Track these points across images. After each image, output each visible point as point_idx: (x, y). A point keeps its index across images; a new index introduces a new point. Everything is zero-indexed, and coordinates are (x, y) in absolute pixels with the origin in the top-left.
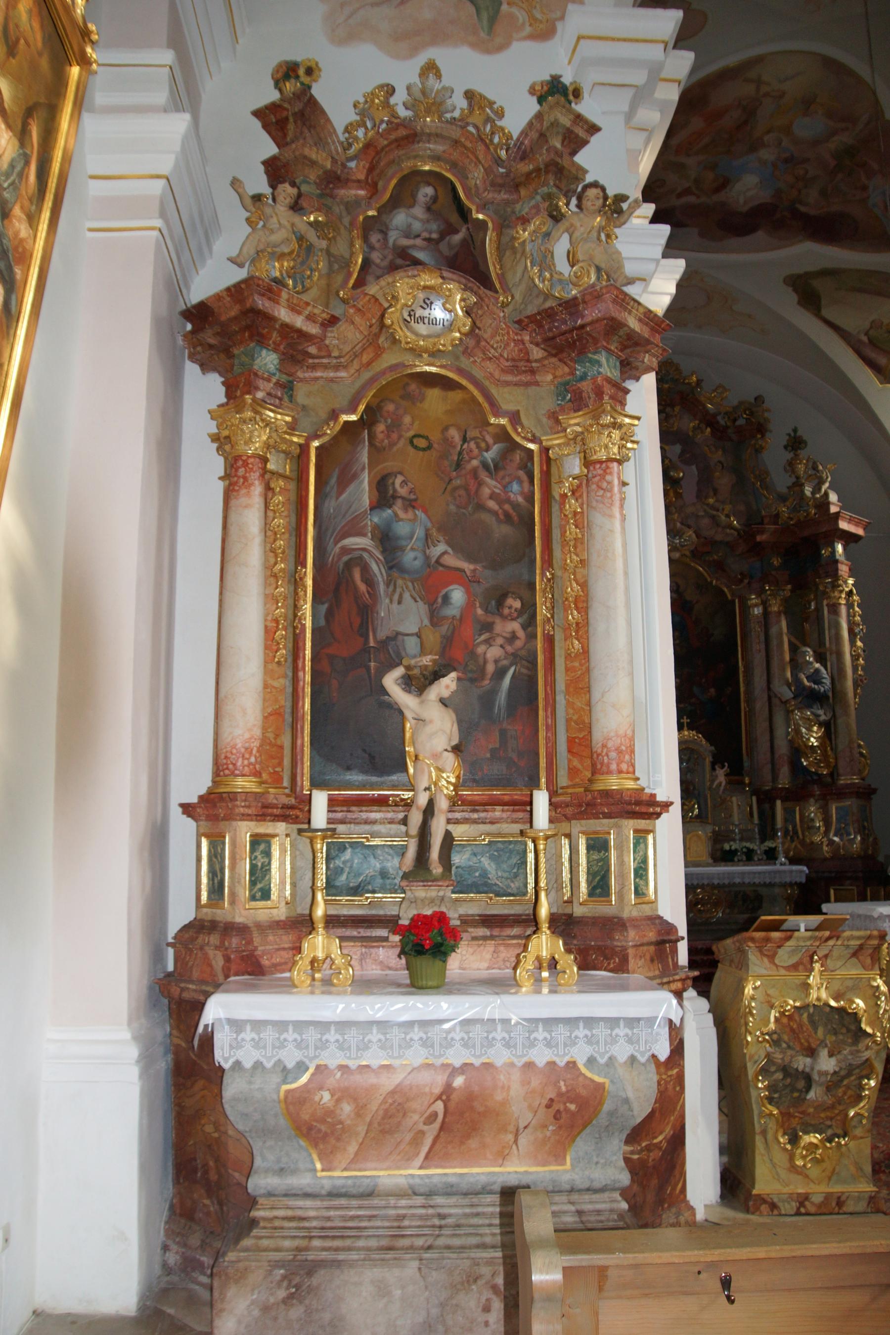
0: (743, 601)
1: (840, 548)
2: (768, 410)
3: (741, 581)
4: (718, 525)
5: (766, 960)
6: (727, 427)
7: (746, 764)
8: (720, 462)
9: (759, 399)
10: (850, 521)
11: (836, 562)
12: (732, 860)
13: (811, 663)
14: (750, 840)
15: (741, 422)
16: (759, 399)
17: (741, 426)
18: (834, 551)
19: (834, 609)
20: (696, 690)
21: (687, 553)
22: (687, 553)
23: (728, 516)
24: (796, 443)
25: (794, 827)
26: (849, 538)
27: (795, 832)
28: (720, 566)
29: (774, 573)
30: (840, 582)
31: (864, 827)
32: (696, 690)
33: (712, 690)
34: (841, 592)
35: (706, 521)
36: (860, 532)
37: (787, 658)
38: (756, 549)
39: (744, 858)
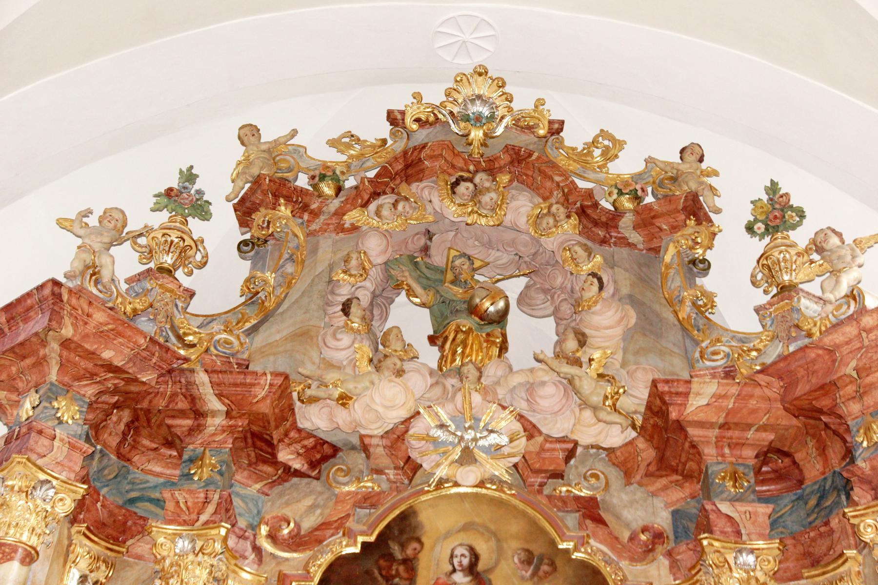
2: (716, 174)
3: (649, 551)
6: (617, 214)
8: (594, 275)
9: (692, 153)
15: (649, 199)
16: (692, 153)
17: (649, 207)
24: (775, 215)
29: (725, 508)
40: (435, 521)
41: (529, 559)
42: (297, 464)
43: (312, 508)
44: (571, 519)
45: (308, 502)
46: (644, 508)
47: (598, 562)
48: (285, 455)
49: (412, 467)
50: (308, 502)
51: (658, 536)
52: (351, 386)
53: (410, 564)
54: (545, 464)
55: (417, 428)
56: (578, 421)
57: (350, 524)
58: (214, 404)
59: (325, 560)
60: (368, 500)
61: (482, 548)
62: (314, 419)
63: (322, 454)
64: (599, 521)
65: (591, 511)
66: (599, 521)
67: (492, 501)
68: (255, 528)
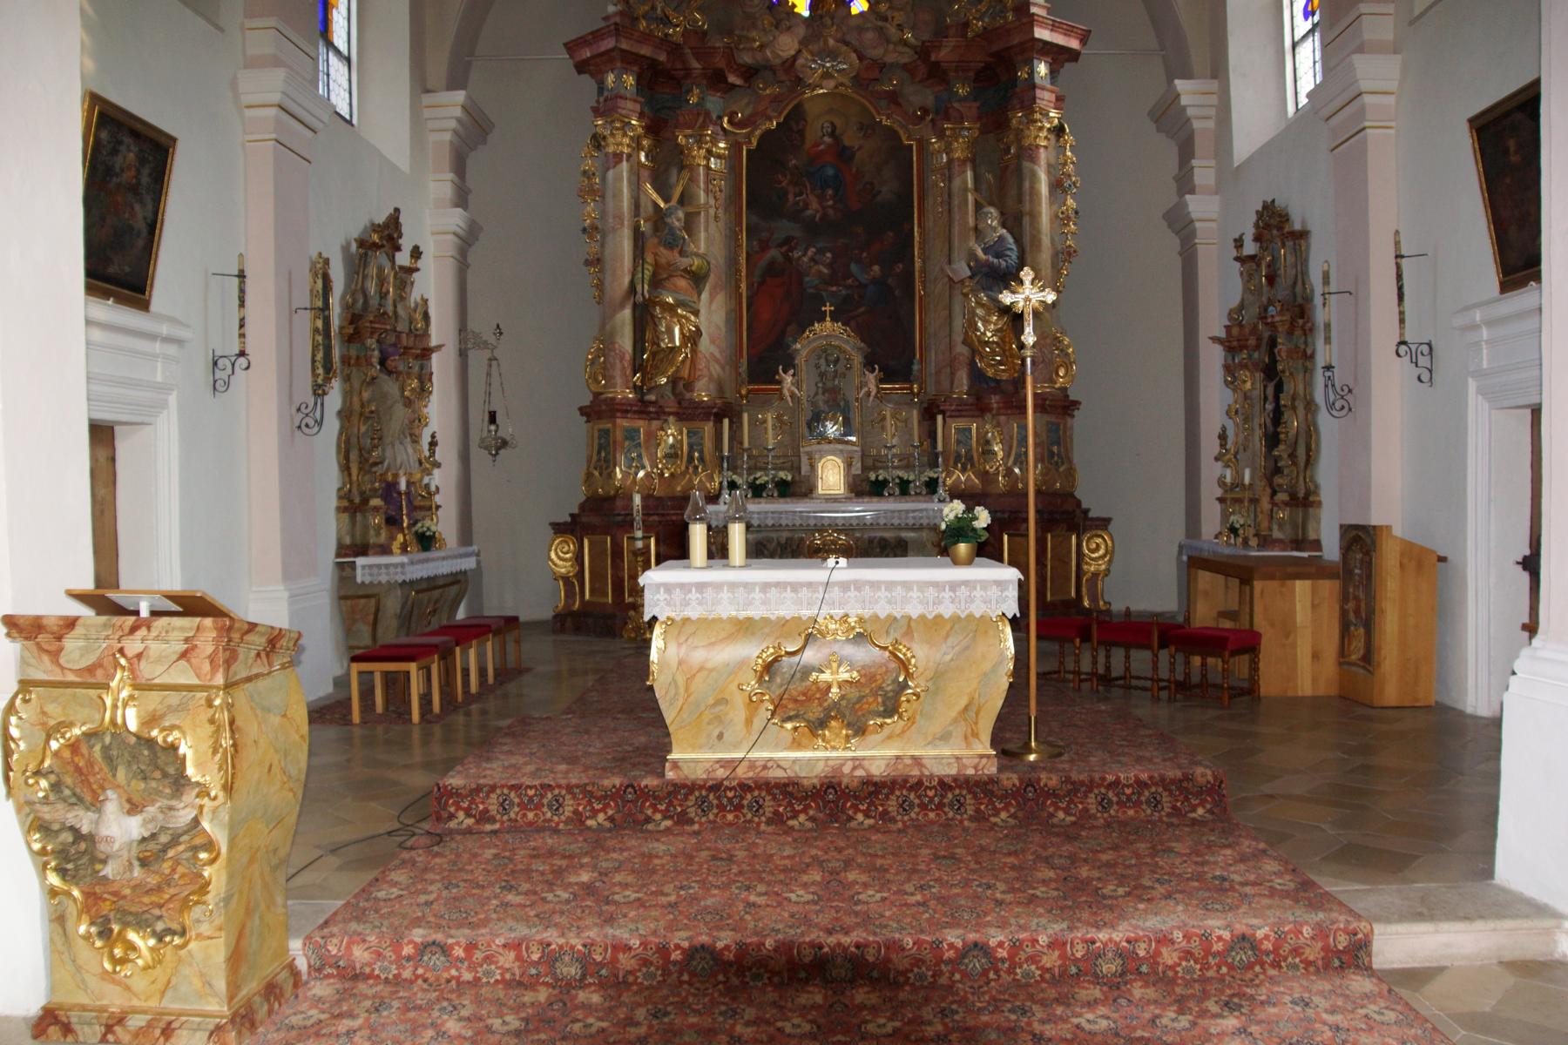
0: (923, 144)
1: (1042, 69)
3: (922, 118)
4: (888, 41)
5: (46, 658)
7: (916, 367)
10: (1054, 27)
11: (1033, 87)
12: (880, 495)
13: (994, 229)
14: (908, 467)
18: (1032, 73)
19: (1029, 153)
20: (854, 268)
21: (845, 81)
22: (845, 81)
23: (900, 27)
25: (969, 451)
26: (1059, 57)
27: (970, 459)
28: (894, 98)
30: (1037, 116)
31: (1052, 454)
32: (854, 268)
33: (876, 268)
34: (1041, 128)
35: (870, 35)
36: (1074, 44)
37: (971, 222)
38: (937, 74)
39: (897, 491)
40: (812, 110)
41: (861, 127)
42: (738, 82)
43: (748, 104)
44: (883, 103)
45: (745, 101)
46: (920, 96)
47: (896, 127)
48: (732, 79)
49: (799, 81)
50: (745, 101)
51: (925, 111)
52: (764, 39)
53: (801, 133)
54: (869, 76)
55: (800, 61)
56: (886, 51)
57: (769, 112)
58: (696, 65)
59: (758, 133)
60: (776, 99)
61: (838, 122)
62: (747, 58)
63: (750, 73)
64: (898, 104)
65: (894, 98)
66: (898, 104)
67: (843, 96)
68: (720, 118)
